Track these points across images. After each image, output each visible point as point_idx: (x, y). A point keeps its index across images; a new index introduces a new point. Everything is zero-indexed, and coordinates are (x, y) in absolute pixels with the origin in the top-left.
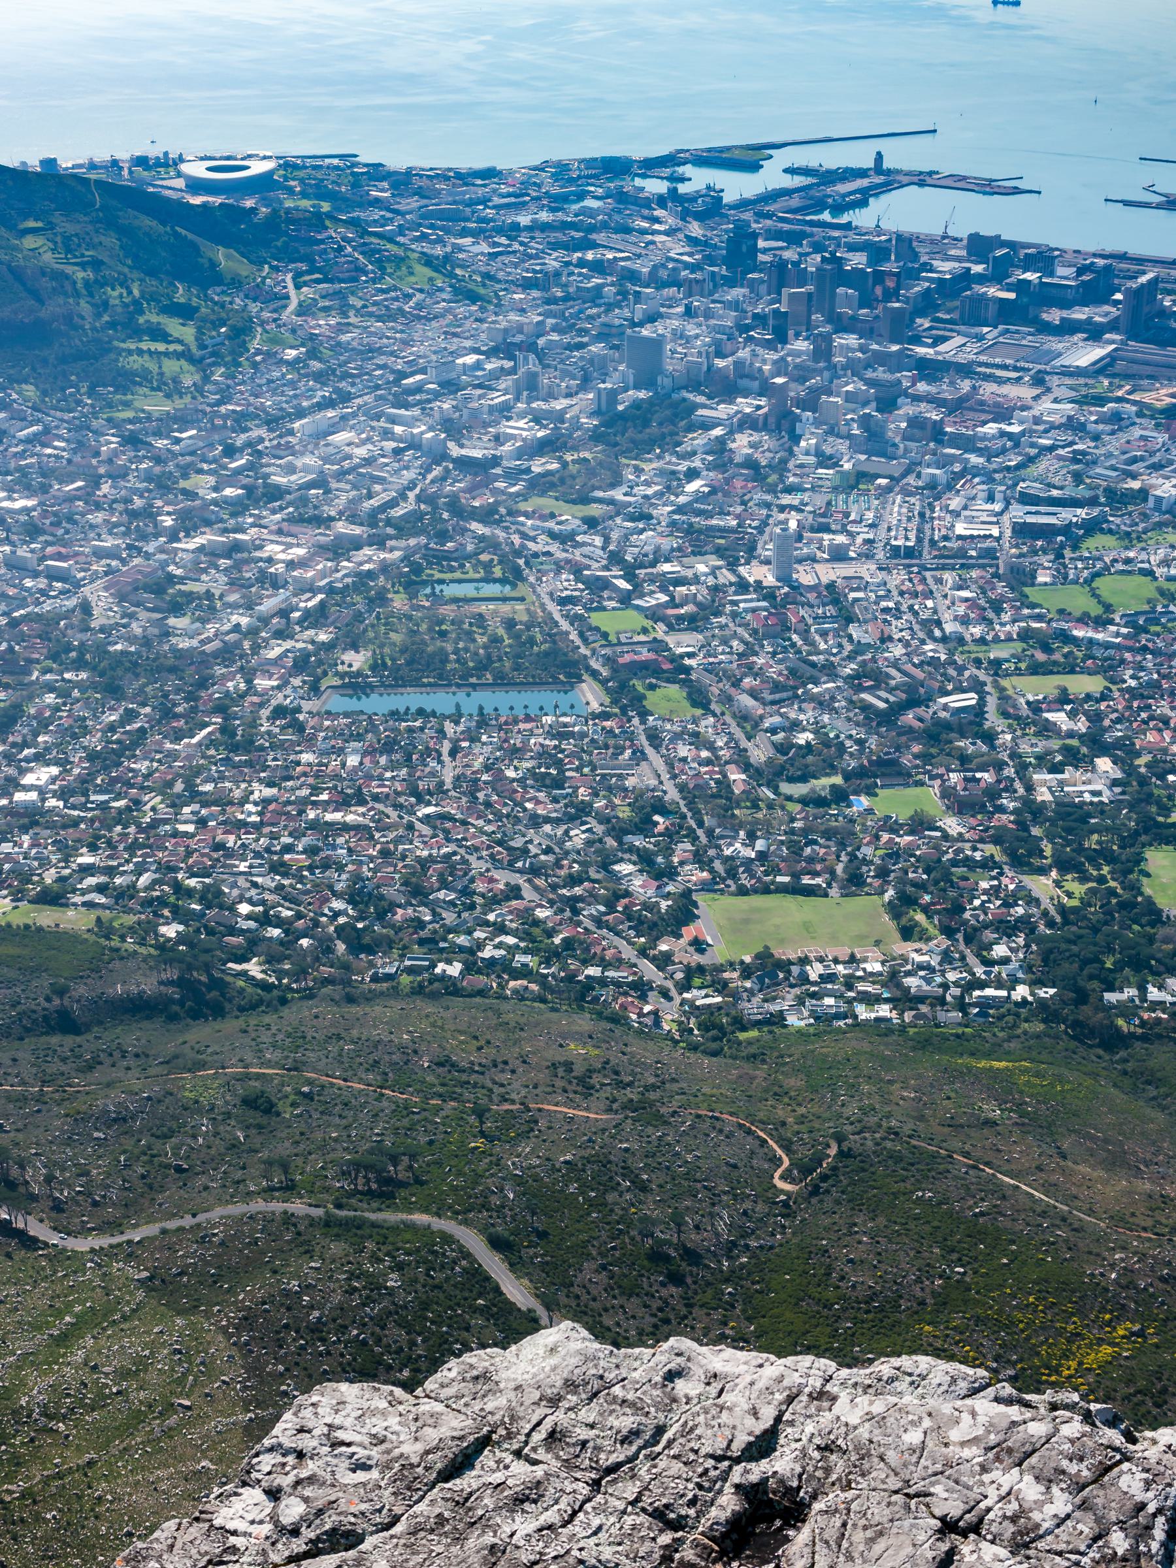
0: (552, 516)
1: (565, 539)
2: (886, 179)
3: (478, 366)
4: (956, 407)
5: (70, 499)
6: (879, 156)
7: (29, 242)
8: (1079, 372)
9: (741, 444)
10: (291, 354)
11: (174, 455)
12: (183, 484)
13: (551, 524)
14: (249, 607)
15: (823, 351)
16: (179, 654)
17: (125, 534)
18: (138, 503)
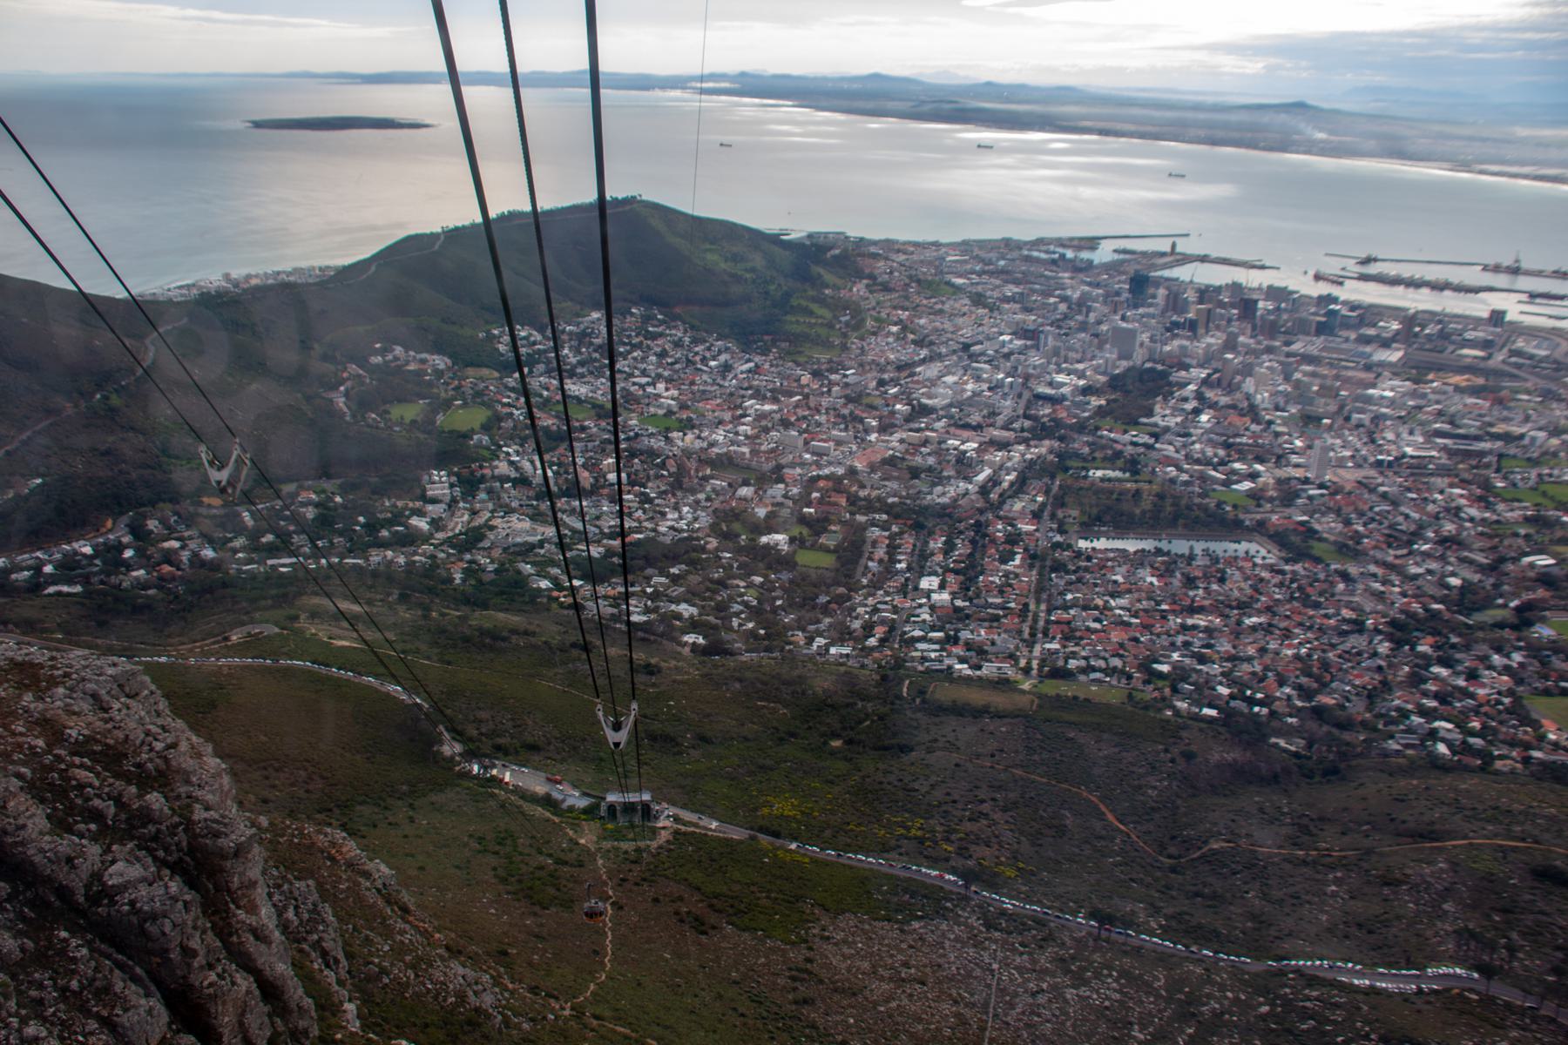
0: (1125, 432)
1: (1149, 447)
2: (1186, 259)
3: (1011, 341)
4: (1337, 377)
5: (797, 406)
6: (1174, 246)
7: (709, 256)
8: (1391, 365)
9: (1209, 394)
10: (894, 329)
11: (847, 385)
12: (865, 401)
13: (1127, 437)
14: (967, 479)
15: (1230, 345)
16: (944, 507)
17: (846, 430)
18: (846, 412)
